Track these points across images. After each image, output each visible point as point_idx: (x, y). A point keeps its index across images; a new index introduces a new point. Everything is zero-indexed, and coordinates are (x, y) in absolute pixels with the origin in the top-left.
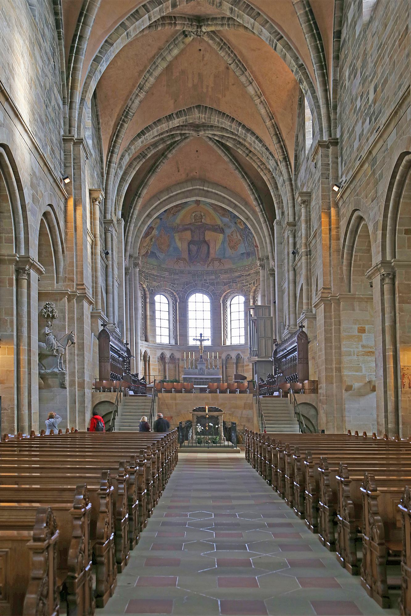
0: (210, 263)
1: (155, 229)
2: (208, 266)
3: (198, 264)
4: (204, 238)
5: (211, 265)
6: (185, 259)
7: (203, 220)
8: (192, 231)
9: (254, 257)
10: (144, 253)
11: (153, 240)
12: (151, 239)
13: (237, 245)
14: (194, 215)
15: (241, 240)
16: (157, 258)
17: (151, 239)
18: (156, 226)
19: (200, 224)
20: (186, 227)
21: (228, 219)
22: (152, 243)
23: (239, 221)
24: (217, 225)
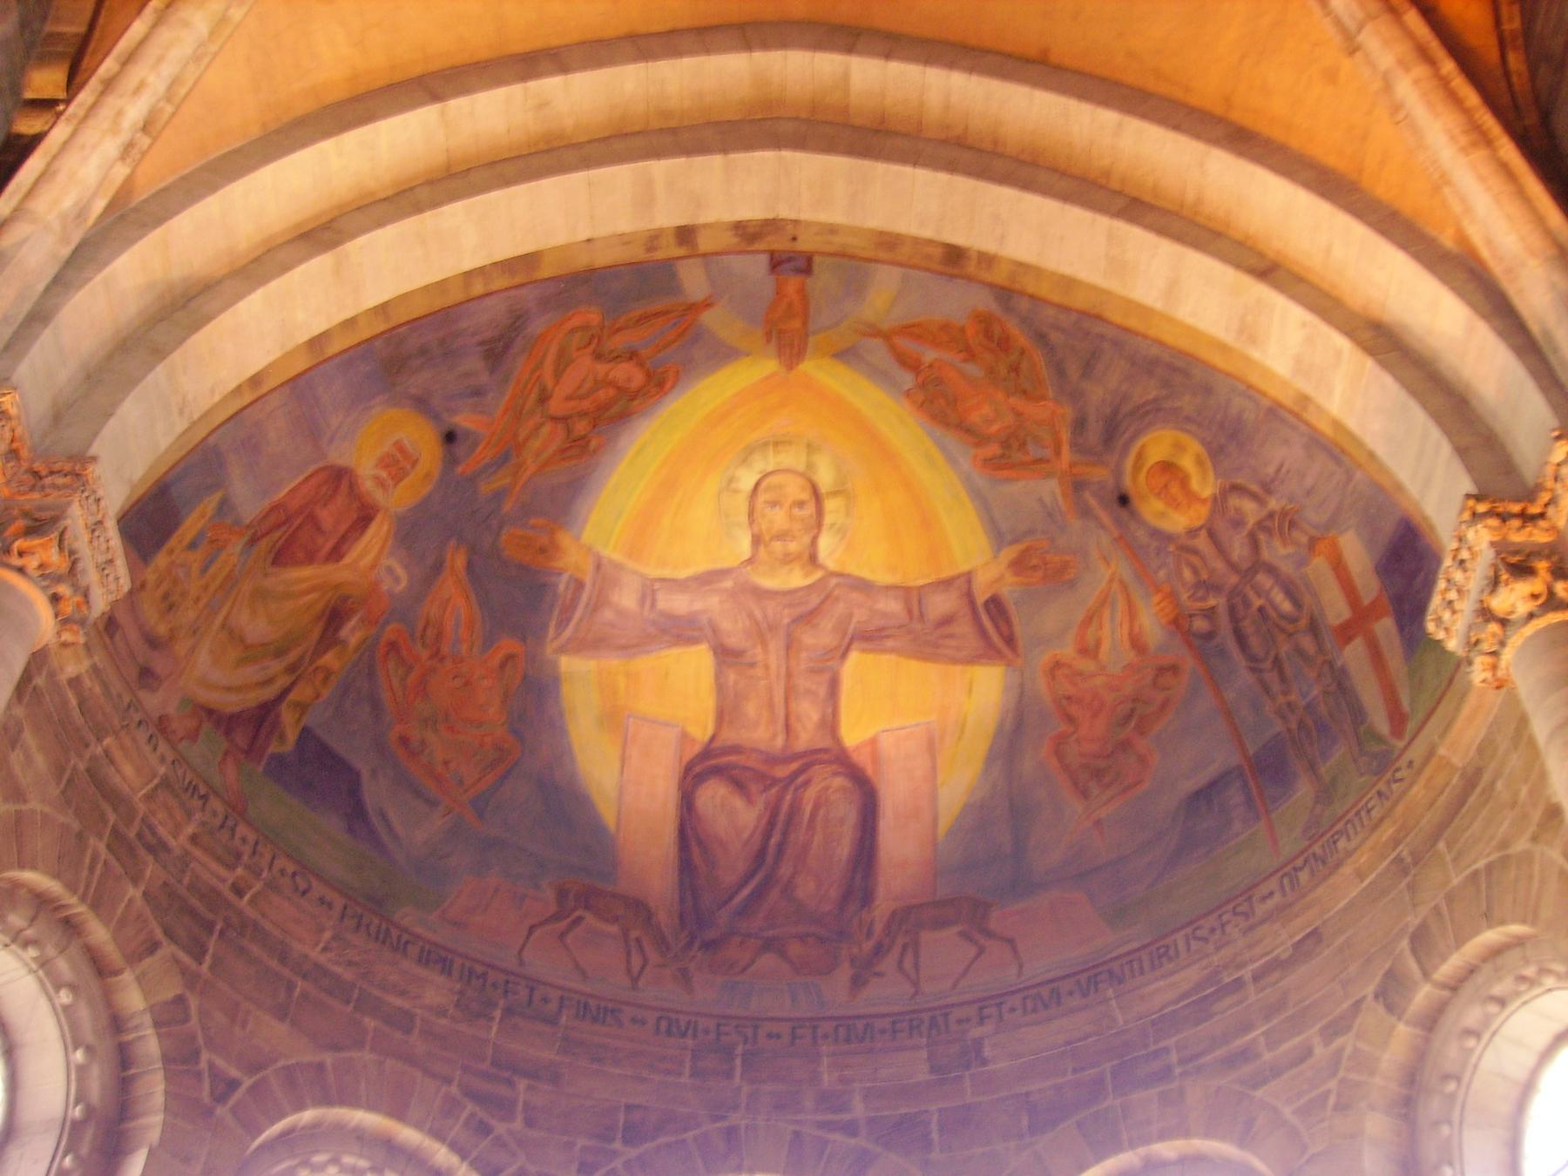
0: (879, 951)
1: (378, 532)
2: (857, 983)
3: (768, 961)
4: (830, 724)
5: (888, 964)
6: (639, 908)
7: (825, 543)
8: (726, 655)
9: (1340, 752)
10: (232, 703)
11: (352, 633)
12: (334, 617)
13: (1141, 730)
14: (747, 480)
15: (1174, 669)
16: (356, 814)
17: (334, 617)
18: (396, 500)
19: (796, 579)
20: (679, 604)
21: (1050, 489)
22: (329, 659)
23: (1158, 444)
24: (946, 584)
